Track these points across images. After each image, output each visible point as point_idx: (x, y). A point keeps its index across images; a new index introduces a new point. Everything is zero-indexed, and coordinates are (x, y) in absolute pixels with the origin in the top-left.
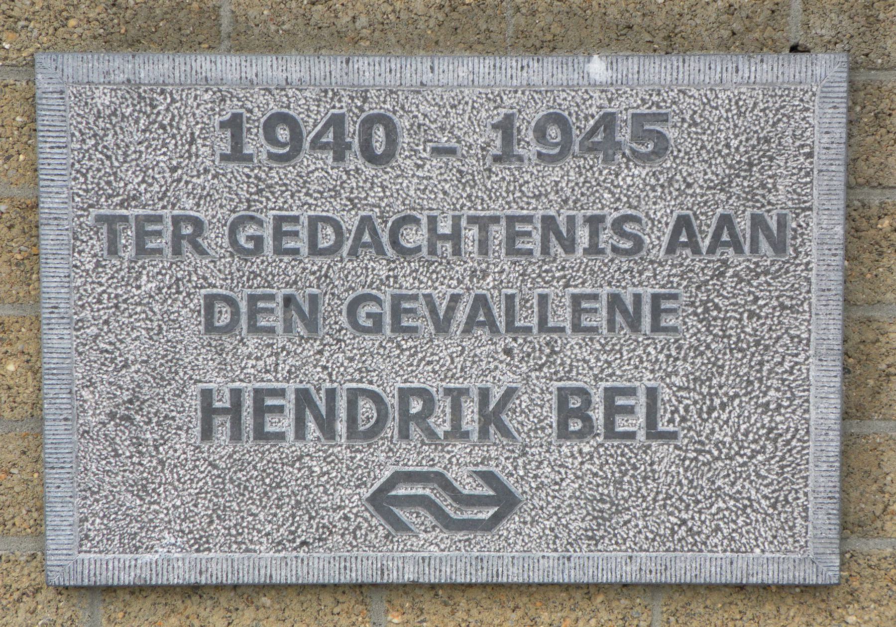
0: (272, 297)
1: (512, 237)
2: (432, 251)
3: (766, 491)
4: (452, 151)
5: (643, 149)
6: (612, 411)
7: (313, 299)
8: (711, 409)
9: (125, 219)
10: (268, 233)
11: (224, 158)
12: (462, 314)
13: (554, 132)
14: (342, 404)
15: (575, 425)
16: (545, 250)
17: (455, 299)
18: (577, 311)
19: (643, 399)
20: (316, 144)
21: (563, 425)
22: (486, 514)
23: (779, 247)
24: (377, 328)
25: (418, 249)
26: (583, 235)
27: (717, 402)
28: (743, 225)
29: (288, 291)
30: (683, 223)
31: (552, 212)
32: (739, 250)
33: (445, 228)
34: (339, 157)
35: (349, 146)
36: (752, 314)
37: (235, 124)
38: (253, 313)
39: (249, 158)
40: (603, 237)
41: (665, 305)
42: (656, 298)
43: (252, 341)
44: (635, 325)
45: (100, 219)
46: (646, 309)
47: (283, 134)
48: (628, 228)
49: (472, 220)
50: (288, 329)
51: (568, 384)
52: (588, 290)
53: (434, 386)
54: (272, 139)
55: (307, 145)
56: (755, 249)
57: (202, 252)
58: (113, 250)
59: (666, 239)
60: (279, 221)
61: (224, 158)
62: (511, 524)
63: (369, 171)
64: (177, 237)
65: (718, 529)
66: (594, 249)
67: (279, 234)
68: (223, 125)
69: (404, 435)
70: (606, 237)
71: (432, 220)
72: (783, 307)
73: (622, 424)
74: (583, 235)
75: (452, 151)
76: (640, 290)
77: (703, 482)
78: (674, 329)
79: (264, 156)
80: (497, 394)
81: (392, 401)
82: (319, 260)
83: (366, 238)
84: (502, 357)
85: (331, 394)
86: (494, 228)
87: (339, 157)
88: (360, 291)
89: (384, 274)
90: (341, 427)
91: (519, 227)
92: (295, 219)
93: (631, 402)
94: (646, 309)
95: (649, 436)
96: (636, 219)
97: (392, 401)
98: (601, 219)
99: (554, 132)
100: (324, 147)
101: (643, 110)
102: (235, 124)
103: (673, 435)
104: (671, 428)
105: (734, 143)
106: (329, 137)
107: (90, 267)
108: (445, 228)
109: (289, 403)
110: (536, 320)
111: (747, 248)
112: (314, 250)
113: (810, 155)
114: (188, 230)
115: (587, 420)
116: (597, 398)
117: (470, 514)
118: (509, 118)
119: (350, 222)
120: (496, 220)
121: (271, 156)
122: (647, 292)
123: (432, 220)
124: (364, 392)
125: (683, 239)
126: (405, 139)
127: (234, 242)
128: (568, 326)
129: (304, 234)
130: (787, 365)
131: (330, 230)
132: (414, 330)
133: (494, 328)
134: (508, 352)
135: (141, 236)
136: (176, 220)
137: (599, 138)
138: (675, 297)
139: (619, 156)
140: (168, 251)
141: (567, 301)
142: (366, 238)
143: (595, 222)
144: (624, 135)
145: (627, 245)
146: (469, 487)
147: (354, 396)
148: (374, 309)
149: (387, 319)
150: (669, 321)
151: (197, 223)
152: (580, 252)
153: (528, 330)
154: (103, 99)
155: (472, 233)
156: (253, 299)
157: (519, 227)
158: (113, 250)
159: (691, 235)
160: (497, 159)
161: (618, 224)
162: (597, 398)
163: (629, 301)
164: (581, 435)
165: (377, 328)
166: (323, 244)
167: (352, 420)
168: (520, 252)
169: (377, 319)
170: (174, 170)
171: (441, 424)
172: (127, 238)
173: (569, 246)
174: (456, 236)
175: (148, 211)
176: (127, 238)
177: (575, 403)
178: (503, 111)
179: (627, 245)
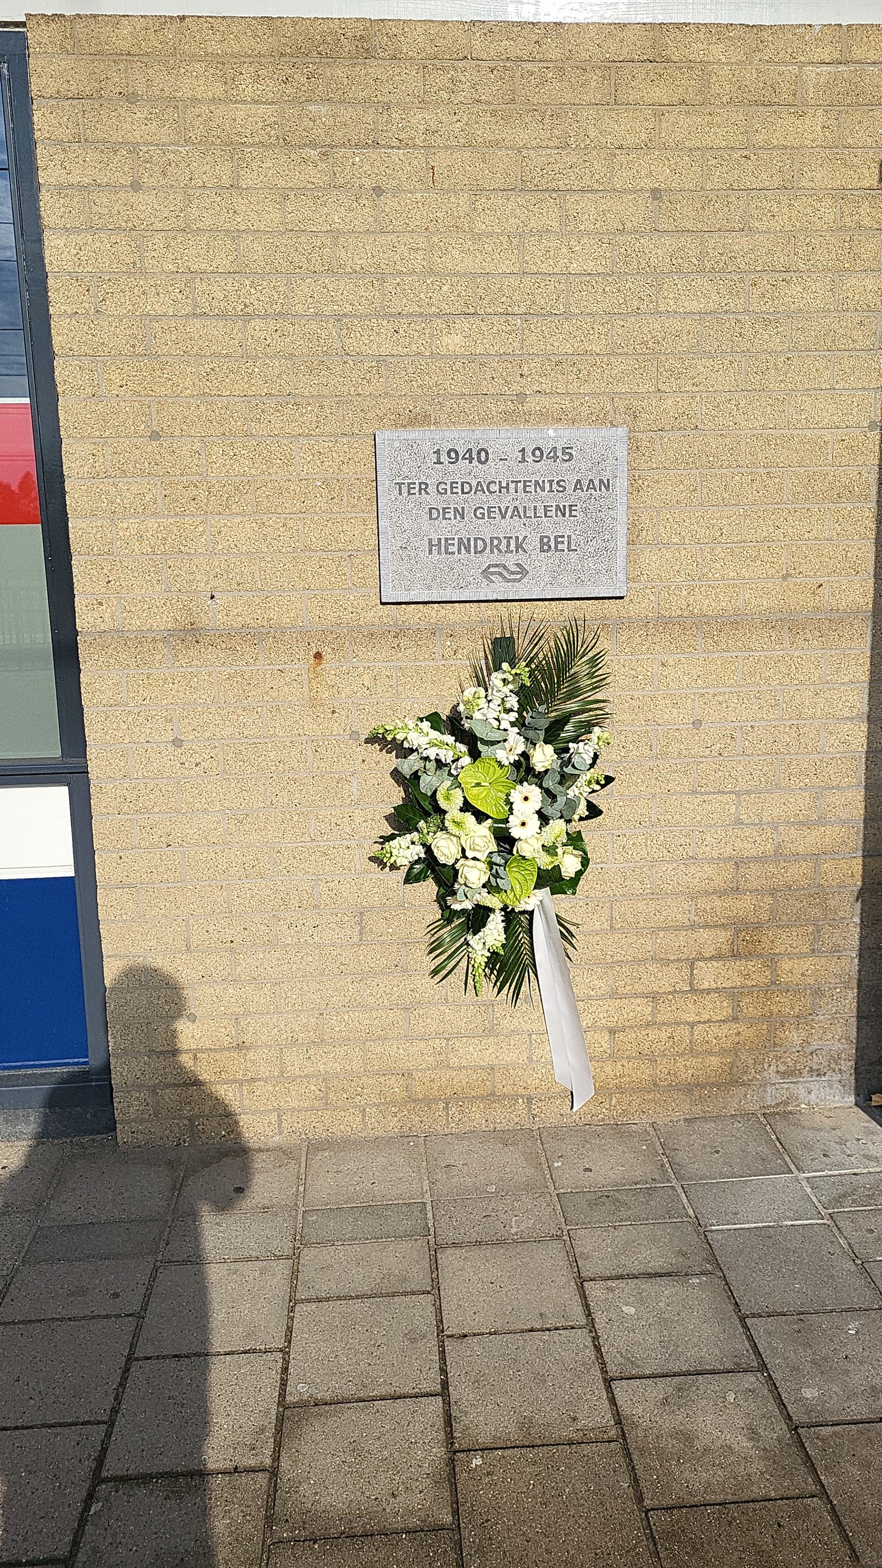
0: (450, 508)
1: (525, 486)
2: (500, 492)
3: (604, 567)
4: (506, 459)
5: (565, 458)
6: (557, 543)
7: (463, 508)
8: (588, 541)
9: (404, 484)
10: (448, 487)
11: (434, 463)
12: (509, 514)
13: (538, 453)
14: (472, 542)
15: (546, 548)
16: (536, 491)
17: (508, 508)
18: (546, 512)
19: (566, 539)
20: (464, 458)
21: (541, 547)
22: (518, 577)
23: (607, 488)
24: (483, 518)
25: (496, 492)
26: (547, 485)
27: (589, 540)
28: (597, 483)
29: (455, 506)
30: (579, 481)
31: (538, 479)
32: (596, 491)
33: (504, 485)
34: (470, 462)
35: (474, 459)
36: (600, 511)
37: (438, 452)
38: (444, 513)
39: (442, 463)
40: (553, 487)
41: (573, 508)
42: (571, 506)
43: (444, 522)
44: (564, 515)
45: (395, 484)
46: (567, 510)
47: (453, 455)
48: (561, 483)
49: (512, 482)
50: (455, 518)
51: (542, 534)
52: (549, 504)
53: (501, 536)
54: (449, 456)
55: (460, 458)
56: (600, 490)
57: (428, 493)
58: (400, 494)
59: (573, 487)
60: (452, 483)
61: (434, 463)
62: (525, 580)
63: (480, 466)
64: (420, 489)
65: (590, 580)
66: (551, 491)
67: (452, 488)
68: (434, 453)
69: (492, 552)
70: (554, 486)
71: (500, 482)
72: (609, 508)
73: (560, 547)
74: (547, 485)
75: (506, 459)
76: (565, 504)
77: (585, 565)
78: (576, 516)
79: (447, 462)
80: (521, 539)
81: (488, 541)
82: (464, 495)
83: (479, 488)
84: (523, 526)
85: (469, 539)
86: (519, 484)
87: (470, 462)
88: (478, 506)
89: (485, 500)
90: (472, 550)
91: (528, 484)
92: (457, 483)
93: (563, 540)
94: (567, 510)
95: (569, 551)
96: (564, 481)
97: (488, 541)
98: (553, 481)
99: (538, 453)
100: (466, 459)
101: (565, 446)
102: (438, 452)
103: (576, 550)
104: (575, 548)
105: (593, 456)
106: (467, 456)
107: (393, 499)
108: (504, 485)
109: (456, 542)
110: (533, 514)
111: (598, 489)
112: (463, 492)
113: (617, 460)
114: (423, 486)
115: (550, 547)
116: (552, 539)
117: (513, 577)
118: (524, 449)
119: (474, 484)
120: (520, 481)
121: (449, 462)
122: (567, 504)
123: (500, 482)
124: (479, 538)
125: (578, 487)
126: (490, 456)
127: (438, 491)
128: (543, 516)
129: (460, 487)
130: (610, 527)
131: (468, 486)
132: (495, 518)
133: (520, 517)
134: (525, 525)
135: (409, 489)
136: (420, 484)
137: (552, 454)
138: (576, 506)
139: (558, 460)
140: (418, 494)
141: (543, 507)
142: (479, 488)
143: (551, 482)
144: (559, 454)
145: (562, 489)
146: (514, 568)
147: (476, 539)
148: (483, 511)
149: (486, 515)
150: (574, 513)
151: (427, 484)
152: (546, 491)
153: (530, 517)
154: (396, 444)
155: (512, 486)
156: (444, 509)
157: (528, 484)
158: (400, 494)
159: (581, 485)
160: (519, 462)
161: (558, 483)
162: (552, 539)
163: (561, 507)
164: (548, 551)
165: (483, 518)
166: (465, 491)
167: (476, 547)
168: (528, 492)
169: (483, 514)
170: (419, 467)
171: (503, 547)
172: (405, 489)
173: (543, 490)
174: (507, 487)
175: (411, 481)
176: (405, 489)
177: (545, 540)
178: (522, 447)
179: (562, 489)
